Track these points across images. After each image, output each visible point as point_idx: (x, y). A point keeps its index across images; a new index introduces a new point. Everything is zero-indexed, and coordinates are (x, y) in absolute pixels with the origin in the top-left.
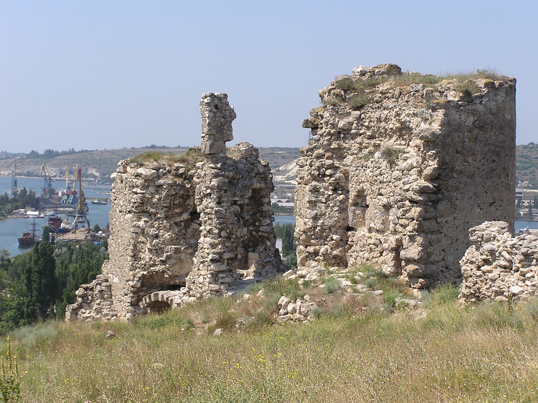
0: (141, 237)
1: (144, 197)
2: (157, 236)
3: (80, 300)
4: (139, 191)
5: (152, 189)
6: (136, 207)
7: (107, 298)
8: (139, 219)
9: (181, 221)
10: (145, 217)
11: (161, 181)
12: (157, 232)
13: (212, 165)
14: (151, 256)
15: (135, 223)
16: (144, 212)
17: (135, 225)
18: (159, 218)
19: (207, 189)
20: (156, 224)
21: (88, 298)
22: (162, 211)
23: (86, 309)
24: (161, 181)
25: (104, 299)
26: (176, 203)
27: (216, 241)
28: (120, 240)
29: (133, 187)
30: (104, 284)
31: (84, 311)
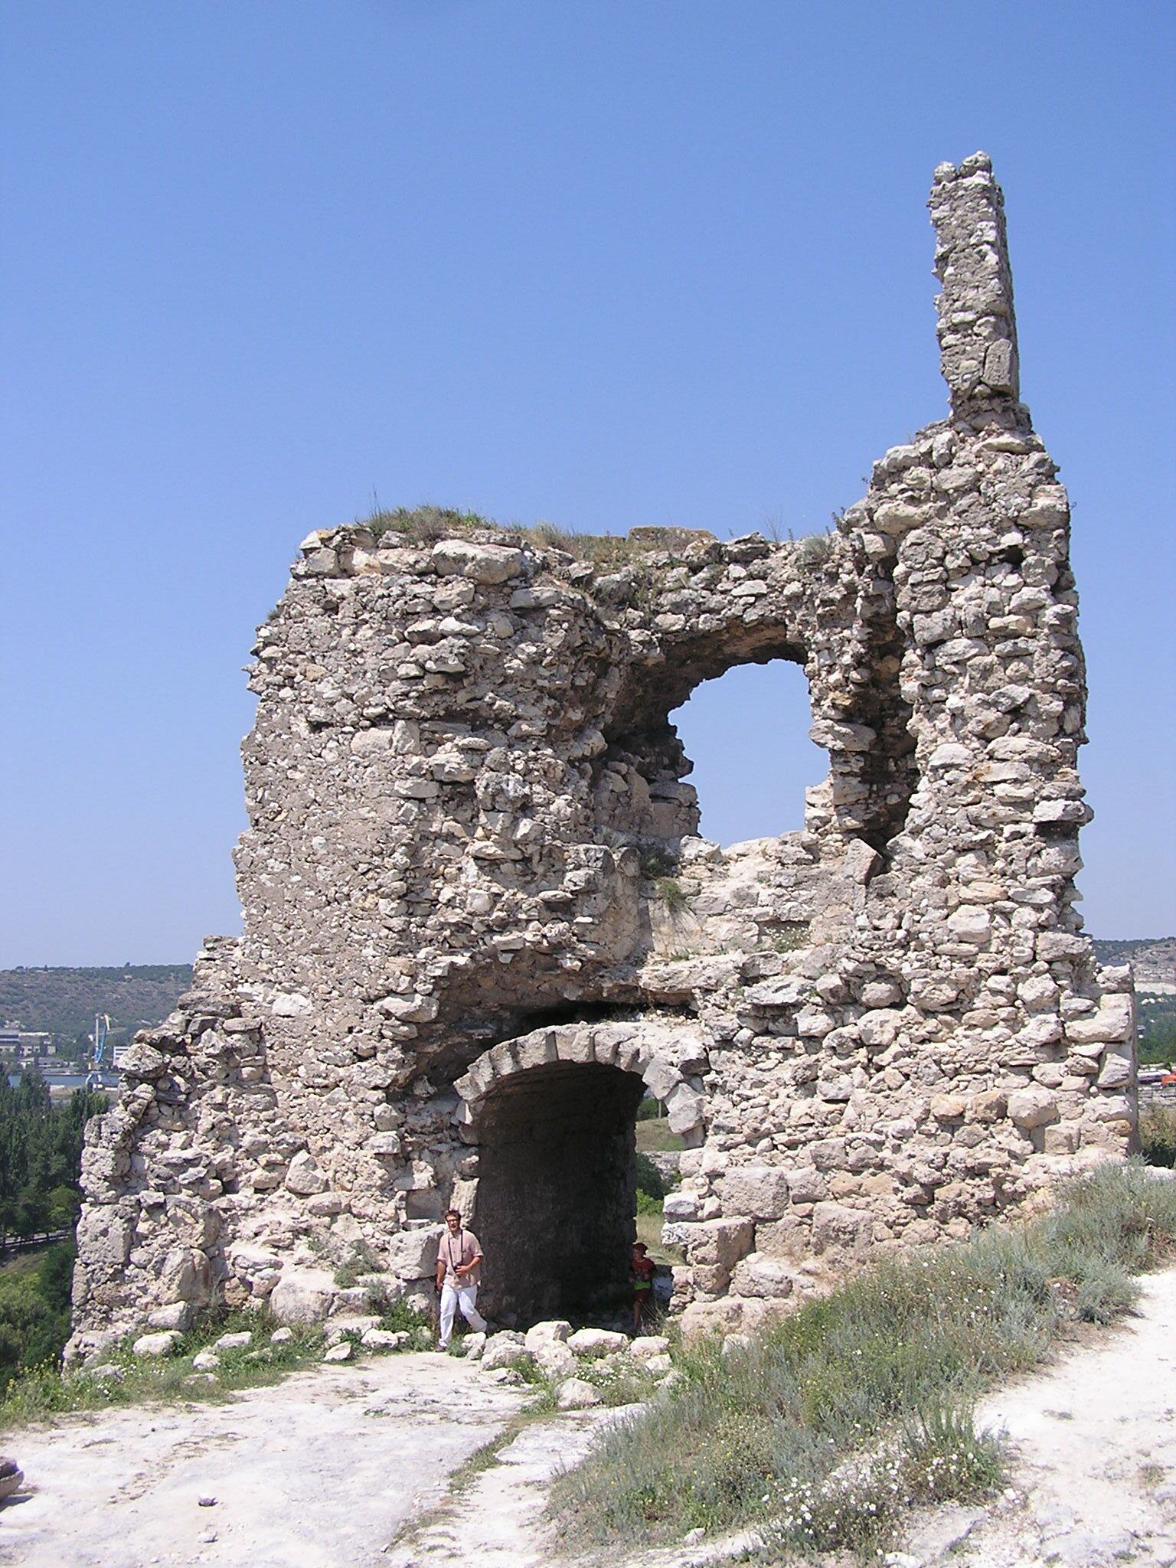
0: (441, 816)
1: (472, 650)
2: (525, 807)
3: (145, 1091)
4: (450, 624)
5: (500, 624)
6: (421, 696)
7: (250, 1079)
8: (431, 744)
9: (584, 759)
10: (457, 732)
11: (542, 591)
12: (527, 790)
13: (1006, 439)
14: (494, 890)
15: (415, 760)
16: (452, 716)
17: (419, 766)
18: (524, 738)
19: (1001, 531)
20: (518, 758)
21: (174, 1084)
22: (536, 711)
23: (168, 1132)
24: (542, 591)
25: (239, 1082)
26: (580, 682)
27: (1055, 753)
28: (316, 841)
29: (408, 616)
30: (232, 1023)
31: (163, 1138)
